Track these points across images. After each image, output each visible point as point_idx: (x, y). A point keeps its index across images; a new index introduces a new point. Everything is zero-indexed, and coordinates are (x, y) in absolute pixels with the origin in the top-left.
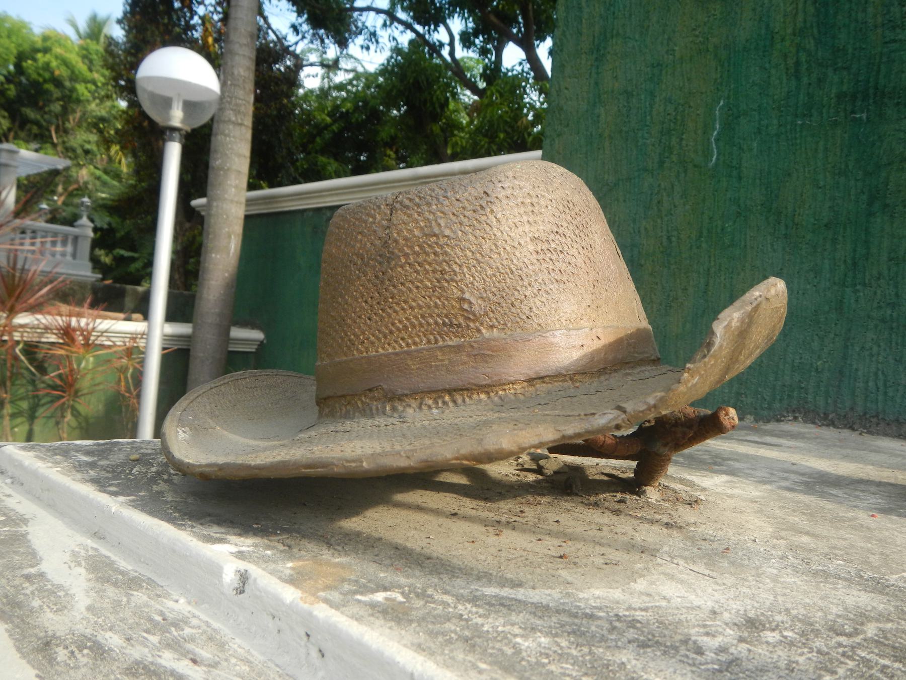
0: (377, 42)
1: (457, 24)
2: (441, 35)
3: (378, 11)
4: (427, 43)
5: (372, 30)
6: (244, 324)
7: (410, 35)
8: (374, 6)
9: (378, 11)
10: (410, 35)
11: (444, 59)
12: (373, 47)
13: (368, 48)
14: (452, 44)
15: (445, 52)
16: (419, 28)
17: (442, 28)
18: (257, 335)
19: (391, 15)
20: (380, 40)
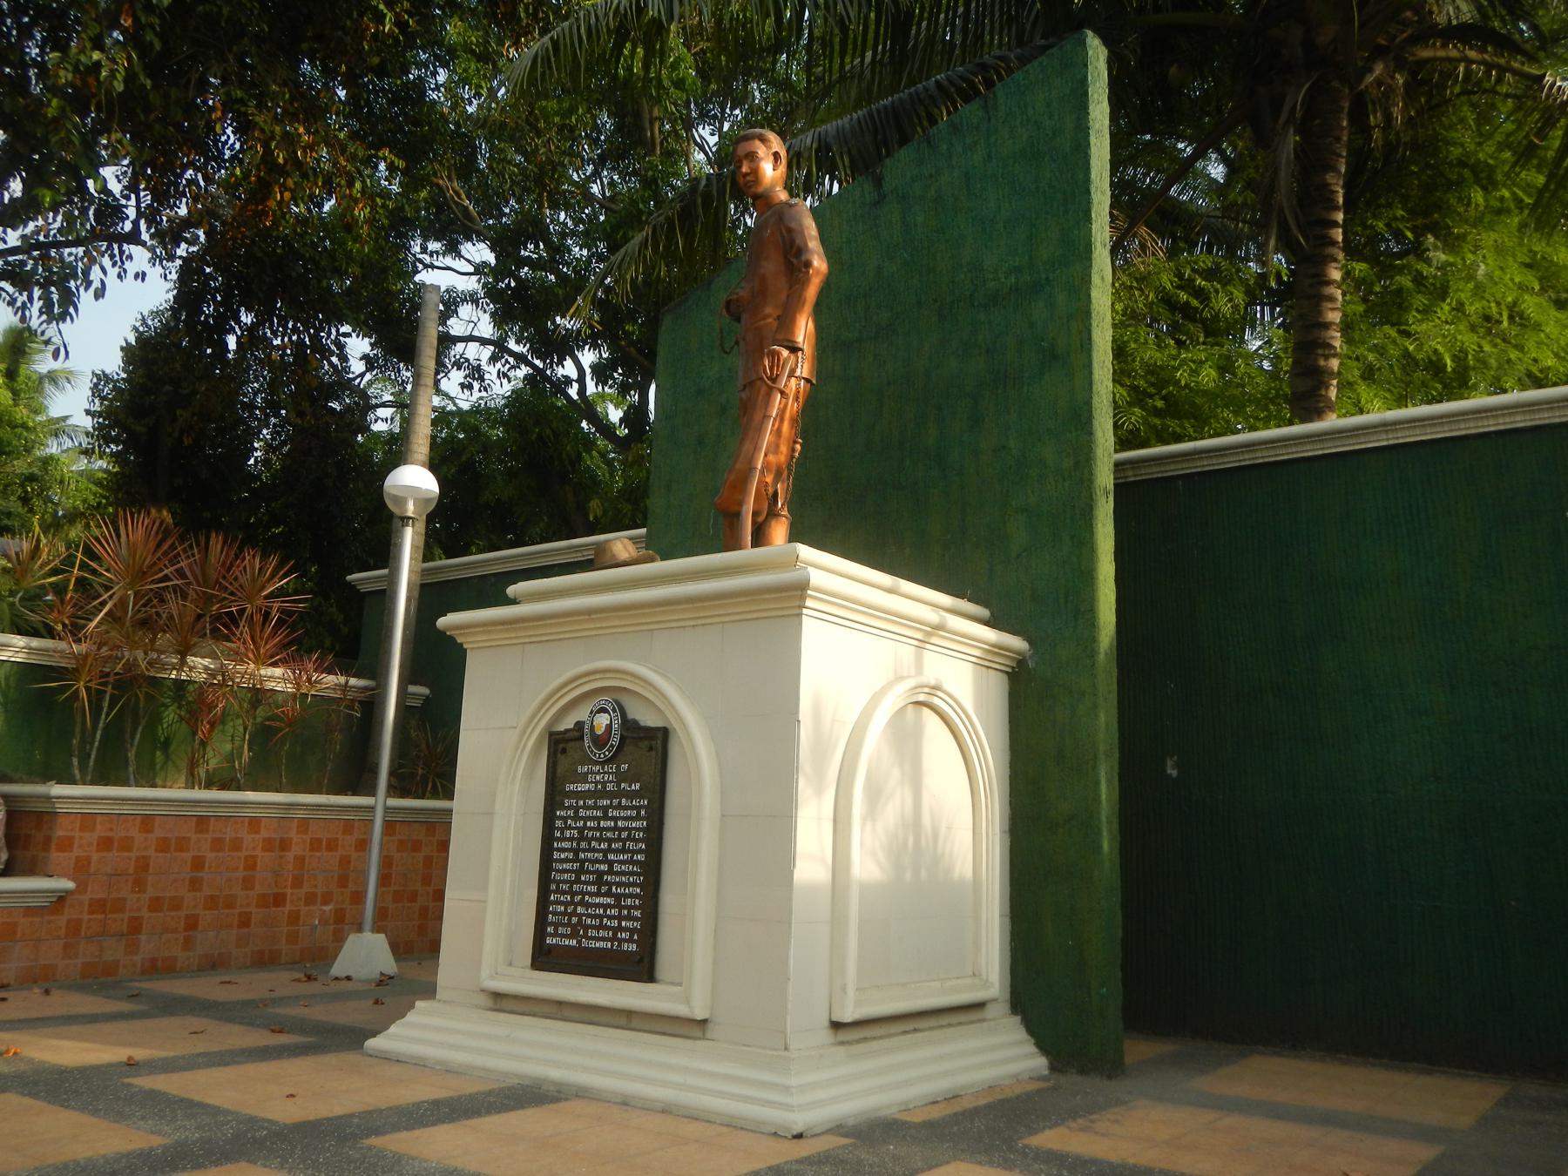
0: (483, 380)
1: (588, 357)
2: (568, 369)
3: (484, 342)
4: (549, 379)
5: (475, 363)
6: (414, 683)
7: (524, 370)
8: (476, 333)
9: (484, 342)
10: (524, 370)
11: (568, 397)
12: (476, 385)
13: (470, 387)
14: (581, 380)
15: (573, 392)
16: (537, 362)
17: (569, 363)
18: (425, 691)
19: (500, 349)
20: (487, 376)
